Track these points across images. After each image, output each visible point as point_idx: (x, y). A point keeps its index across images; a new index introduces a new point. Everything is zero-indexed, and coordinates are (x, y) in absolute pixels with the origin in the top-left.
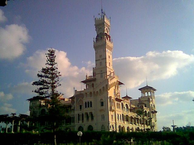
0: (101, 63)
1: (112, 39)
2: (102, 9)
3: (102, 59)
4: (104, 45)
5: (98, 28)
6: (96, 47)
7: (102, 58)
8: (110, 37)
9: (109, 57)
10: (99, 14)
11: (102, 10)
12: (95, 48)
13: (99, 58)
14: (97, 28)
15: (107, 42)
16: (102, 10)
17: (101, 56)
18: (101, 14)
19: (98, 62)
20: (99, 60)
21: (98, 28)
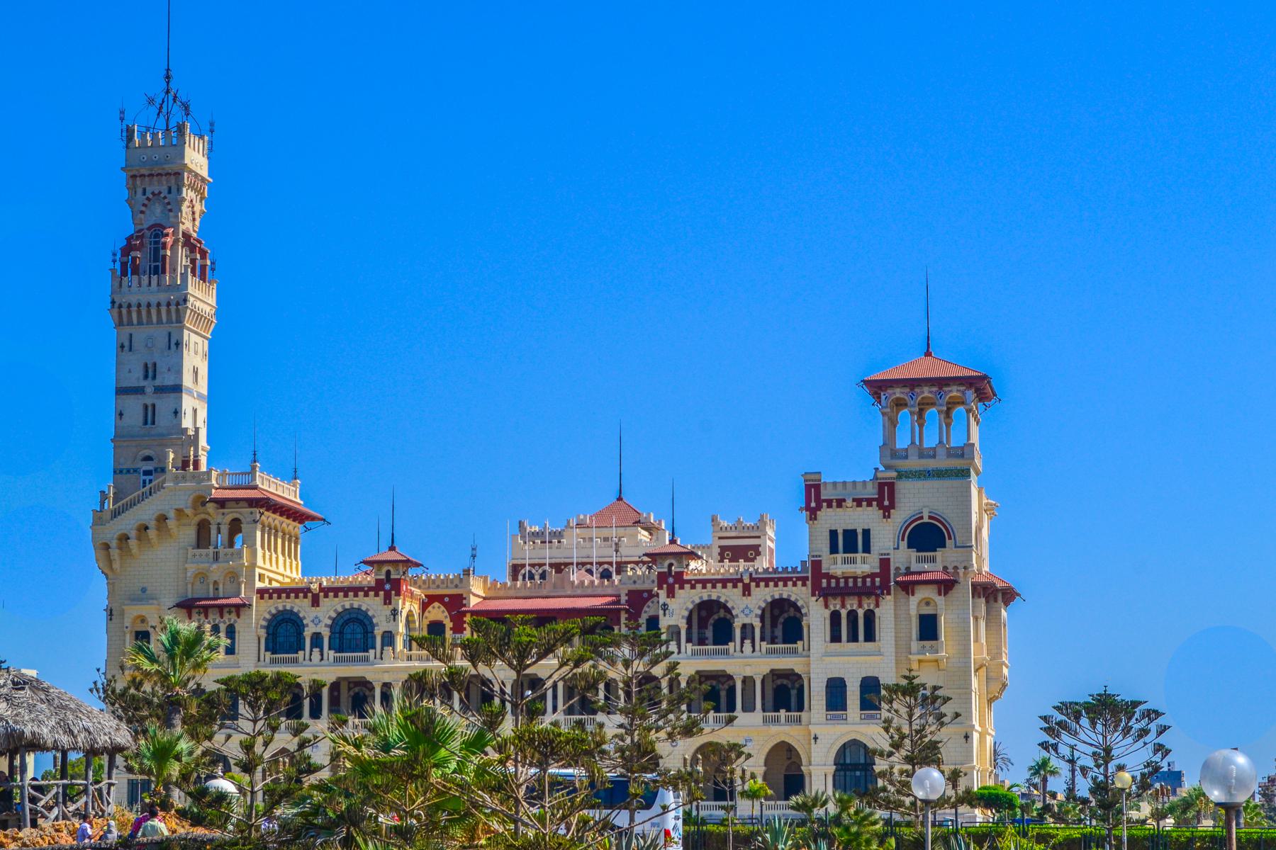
0: (149, 415)
2: (168, 70)
3: (160, 390)
4: (178, 311)
5: (144, 193)
6: (123, 313)
7: (158, 382)
11: (168, 77)
13: (135, 379)
16: (168, 77)
17: (150, 371)
19: (134, 406)
20: (139, 391)
21: (144, 193)
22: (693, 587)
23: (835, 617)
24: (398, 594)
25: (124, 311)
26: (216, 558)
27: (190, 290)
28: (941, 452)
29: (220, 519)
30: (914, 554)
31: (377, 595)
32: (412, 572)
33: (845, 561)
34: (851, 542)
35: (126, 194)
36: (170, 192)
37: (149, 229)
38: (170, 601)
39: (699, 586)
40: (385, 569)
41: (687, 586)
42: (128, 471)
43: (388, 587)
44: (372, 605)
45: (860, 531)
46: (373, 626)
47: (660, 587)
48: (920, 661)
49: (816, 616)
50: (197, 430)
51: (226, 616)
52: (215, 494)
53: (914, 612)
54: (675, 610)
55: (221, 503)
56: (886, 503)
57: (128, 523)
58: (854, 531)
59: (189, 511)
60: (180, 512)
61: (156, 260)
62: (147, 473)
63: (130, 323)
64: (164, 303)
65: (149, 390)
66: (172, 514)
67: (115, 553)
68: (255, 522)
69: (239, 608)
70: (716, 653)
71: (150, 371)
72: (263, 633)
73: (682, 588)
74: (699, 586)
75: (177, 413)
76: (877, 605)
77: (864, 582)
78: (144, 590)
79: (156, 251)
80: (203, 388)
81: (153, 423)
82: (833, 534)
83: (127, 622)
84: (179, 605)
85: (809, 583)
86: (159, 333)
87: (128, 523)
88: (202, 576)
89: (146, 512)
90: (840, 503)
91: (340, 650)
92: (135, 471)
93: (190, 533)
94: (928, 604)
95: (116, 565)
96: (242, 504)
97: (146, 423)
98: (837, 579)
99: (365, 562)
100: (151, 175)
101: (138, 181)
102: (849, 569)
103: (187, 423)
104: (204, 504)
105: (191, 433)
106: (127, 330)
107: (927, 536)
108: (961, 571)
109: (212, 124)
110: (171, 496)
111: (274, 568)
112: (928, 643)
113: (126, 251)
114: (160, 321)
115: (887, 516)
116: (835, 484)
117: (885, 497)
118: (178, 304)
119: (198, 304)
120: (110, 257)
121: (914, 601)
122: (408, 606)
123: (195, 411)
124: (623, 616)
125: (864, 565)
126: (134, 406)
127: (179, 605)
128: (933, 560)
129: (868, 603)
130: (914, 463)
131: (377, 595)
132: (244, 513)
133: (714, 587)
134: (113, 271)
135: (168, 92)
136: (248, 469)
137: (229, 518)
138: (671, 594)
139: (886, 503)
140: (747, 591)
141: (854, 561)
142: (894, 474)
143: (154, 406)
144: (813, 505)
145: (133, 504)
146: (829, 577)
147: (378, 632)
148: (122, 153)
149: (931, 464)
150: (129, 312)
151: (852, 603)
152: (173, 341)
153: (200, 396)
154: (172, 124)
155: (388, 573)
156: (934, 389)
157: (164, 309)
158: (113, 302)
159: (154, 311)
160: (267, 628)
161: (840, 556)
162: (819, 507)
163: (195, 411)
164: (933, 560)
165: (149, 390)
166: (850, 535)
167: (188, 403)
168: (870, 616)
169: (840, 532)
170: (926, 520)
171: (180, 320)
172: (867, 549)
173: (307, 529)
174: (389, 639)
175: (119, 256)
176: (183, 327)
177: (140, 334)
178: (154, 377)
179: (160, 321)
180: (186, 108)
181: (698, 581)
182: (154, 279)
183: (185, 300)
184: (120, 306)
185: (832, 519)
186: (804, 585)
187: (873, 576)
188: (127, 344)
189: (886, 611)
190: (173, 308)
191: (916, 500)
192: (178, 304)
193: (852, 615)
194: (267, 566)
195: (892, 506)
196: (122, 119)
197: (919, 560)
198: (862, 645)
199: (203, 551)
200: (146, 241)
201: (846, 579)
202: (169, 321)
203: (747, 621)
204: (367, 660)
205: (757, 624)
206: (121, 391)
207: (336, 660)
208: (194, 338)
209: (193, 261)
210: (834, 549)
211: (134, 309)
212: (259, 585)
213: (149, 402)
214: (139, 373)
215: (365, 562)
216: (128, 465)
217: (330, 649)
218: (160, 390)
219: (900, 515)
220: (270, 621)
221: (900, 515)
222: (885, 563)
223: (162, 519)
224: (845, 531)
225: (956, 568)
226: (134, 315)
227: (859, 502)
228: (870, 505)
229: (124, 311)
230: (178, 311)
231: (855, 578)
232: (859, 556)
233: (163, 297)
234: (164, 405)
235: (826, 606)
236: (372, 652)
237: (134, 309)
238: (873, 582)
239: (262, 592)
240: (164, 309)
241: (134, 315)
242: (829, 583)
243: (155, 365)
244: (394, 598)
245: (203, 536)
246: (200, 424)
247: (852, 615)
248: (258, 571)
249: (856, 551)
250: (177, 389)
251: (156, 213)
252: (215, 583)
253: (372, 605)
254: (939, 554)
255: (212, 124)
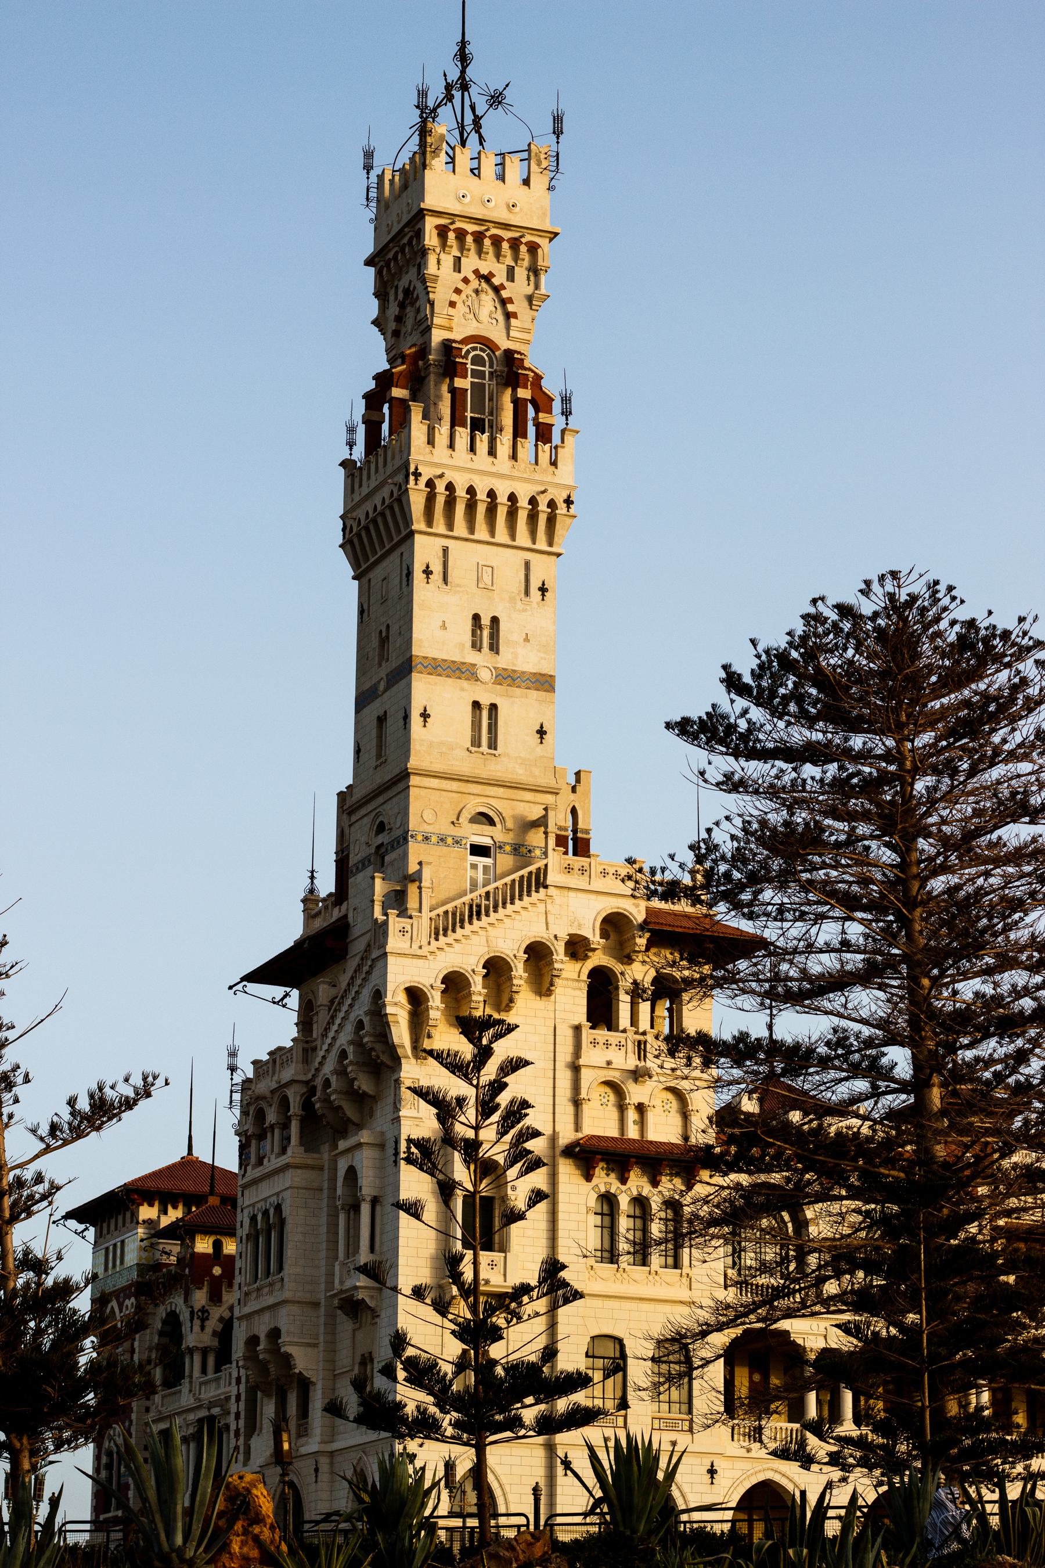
2: (463, 44)
11: (463, 57)
62: (478, 850)
81: (493, 744)
97: (476, 742)
143: (493, 707)
152: (535, 584)
165: (484, 675)
178: (494, 647)
213: (485, 701)
223: (537, 954)
243: (495, 620)
245: (601, 1009)
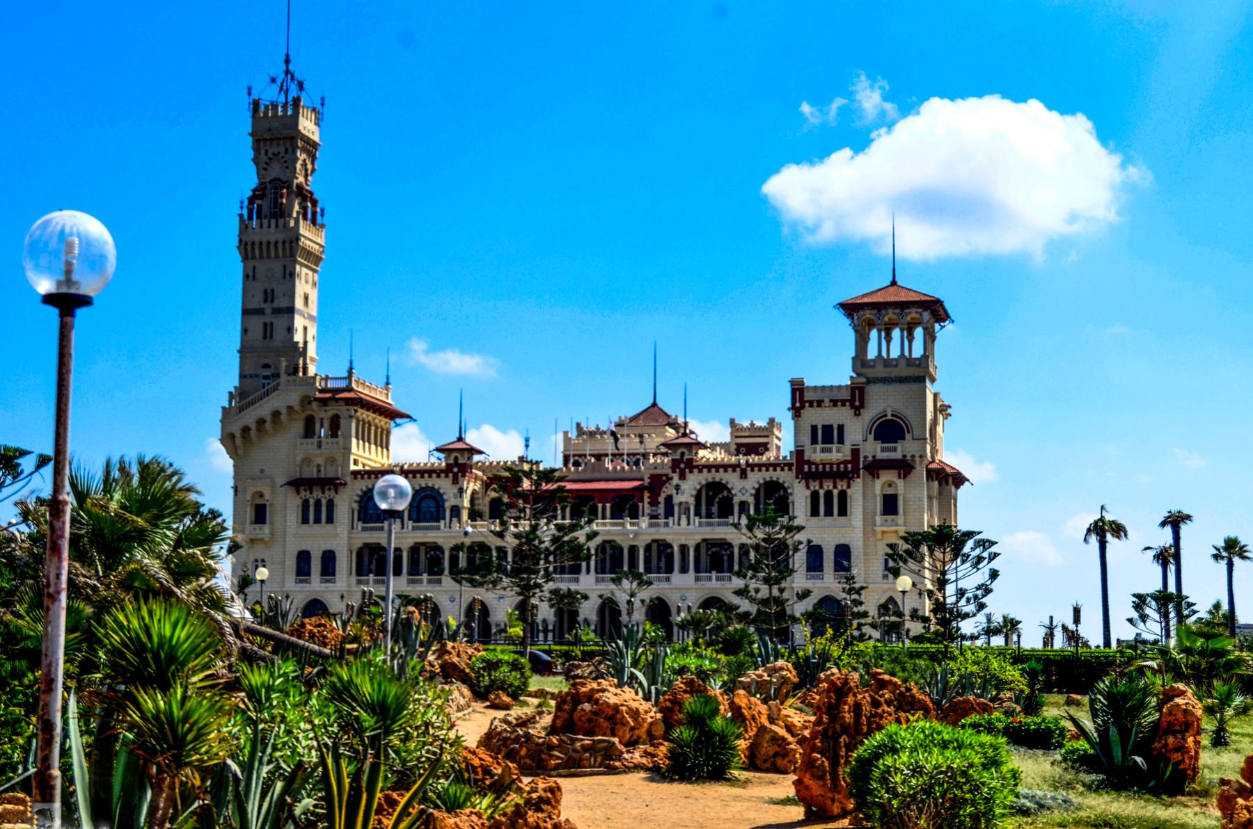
0: (268, 330)
1: (322, 210)
2: (288, 55)
3: (277, 311)
4: (291, 247)
5: (266, 153)
6: (248, 249)
7: (276, 305)
8: (314, 203)
9: (306, 298)
10: (273, 80)
11: (287, 61)
12: (246, 250)
13: (257, 302)
14: (263, 152)
15: (305, 230)
16: (287, 61)
17: (269, 296)
18: (279, 82)
19: (257, 323)
20: (260, 312)
21: (266, 153)
22: (700, 471)
23: (815, 496)
24: (464, 476)
25: (249, 248)
26: (319, 445)
27: (302, 231)
28: (903, 364)
29: (324, 414)
30: (879, 445)
31: (447, 476)
32: (476, 458)
33: (823, 451)
34: (828, 435)
35: (251, 154)
36: (286, 151)
37: (270, 182)
38: (281, 480)
39: (705, 470)
40: (454, 455)
41: (696, 471)
42: (251, 376)
43: (455, 470)
44: (444, 485)
45: (835, 426)
46: (444, 501)
47: (674, 472)
48: (883, 532)
49: (800, 496)
50: (306, 343)
51: (327, 493)
52: (318, 395)
53: (878, 491)
54: (687, 490)
55: (324, 402)
56: (857, 403)
57: (250, 418)
58: (831, 427)
59: (297, 408)
60: (290, 408)
61: (275, 207)
62: (266, 377)
63: (254, 258)
64: (280, 241)
65: (268, 311)
66: (284, 411)
67: (238, 441)
68: (351, 417)
69: (334, 484)
70: (719, 524)
71: (269, 296)
72: (355, 506)
73: (691, 472)
74: (705, 470)
75: (290, 330)
76: (849, 487)
77: (838, 467)
78: (262, 471)
79: (276, 199)
80: (313, 309)
81: (271, 337)
82: (814, 428)
83: (248, 497)
84: (290, 483)
85: (794, 468)
86: (277, 267)
87: (250, 418)
88: (307, 461)
89: (264, 409)
90: (820, 403)
91: (418, 520)
92: (257, 376)
93: (299, 427)
94: (890, 486)
95: (240, 452)
96: (341, 403)
97: (265, 337)
98: (817, 465)
99: (438, 450)
100: (272, 139)
101: (262, 144)
102: (826, 457)
103: (298, 337)
104: (310, 403)
105: (301, 345)
106: (251, 263)
107: (890, 430)
108: (917, 459)
109: (323, 99)
110: (285, 398)
111: (367, 455)
112: (889, 518)
113: (251, 200)
114: (277, 256)
115: (857, 414)
116: (815, 388)
117: (855, 397)
118: (291, 242)
119: (308, 243)
120: (238, 205)
121: (878, 484)
122: (471, 486)
123: (305, 329)
124: (646, 495)
125: (837, 454)
126: (257, 323)
127: (290, 483)
128: (895, 449)
129: (842, 485)
130: (880, 371)
131: (447, 476)
132: (342, 410)
133: (717, 471)
134: (241, 216)
135: (287, 72)
136: (346, 375)
137: (330, 414)
138: (682, 477)
139: (857, 403)
140: (744, 475)
141: (830, 451)
142: (864, 380)
143: (272, 324)
144: (798, 405)
145: (254, 402)
146: (810, 463)
147: (448, 505)
148: (249, 121)
149: (895, 372)
150: (253, 249)
151: (828, 485)
153: (311, 318)
154: (290, 99)
155: (456, 458)
156: (898, 311)
157: (280, 247)
158: (240, 241)
159: (272, 248)
160: (359, 502)
161: (819, 447)
162: (802, 407)
163: (305, 329)
164: (895, 449)
165: (268, 311)
166: (828, 429)
167: (299, 322)
168: (843, 495)
169: (820, 427)
170: (889, 417)
171: (293, 255)
172: (841, 441)
173: (397, 425)
174: (456, 511)
175: (246, 203)
176: (295, 262)
177: (262, 267)
178: (272, 301)
179: (277, 256)
180: (301, 86)
181: (704, 466)
182: (273, 222)
183: (298, 239)
184: (246, 244)
185: (815, 417)
186: (790, 470)
187: (845, 462)
188: (251, 274)
189: (856, 491)
190: (287, 245)
191: (881, 402)
192: (291, 242)
193: (829, 495)
194: (361, 453)
195: (862, 406)
196: (249, 94)
197: (883, 450)
198: (836, 519)
199: (310, 441)
200: (267, 192)
201: (824, 465)
202: (284, 256)
203: (744, 499)
204: (438, 528)
205: (751, 500)
206: (246, 312)
207: (414, 528)
208: (304, 270)
209: (305, 209)
210: (814, 441)
211: (257, 246)
212: (353, 467)
213: (268, 321)
214: (259, 297)
215: (438, 450)
216: (251, 372)
217: (410, 519)
218: (277, 311)
219: (869, 414)
220: (361, 497)
221: (869, 414)
222: (855, 452)
223: (276, 414)
224: (824, 427)
225: (913, 456)
226: (257, 251)
227: (834, 403)
228: (844, 405)
229: (249, 248)
230: (291, 247)
231: (831, 465)
232: (834, 447)
233: (280, 237)
234: (279, 322)
235: (808, 487)
236: (442, 522)
237: (257, 246)
238: (846, 467)
239: (355, 473)
240: (280, 247)
241: (257, 251)
242: (810, 468)
243: (273, 291)
244: (460, 479)
245: (309, 432)
246: (309, 338)
247: (829, 495)
248: (352, 457)
249: (832, 443)
250: (291, 310)
251: (275, 171)
252: (319, 466)
253: (444, 485)
254: (899, 445)
255: (323, 99)
